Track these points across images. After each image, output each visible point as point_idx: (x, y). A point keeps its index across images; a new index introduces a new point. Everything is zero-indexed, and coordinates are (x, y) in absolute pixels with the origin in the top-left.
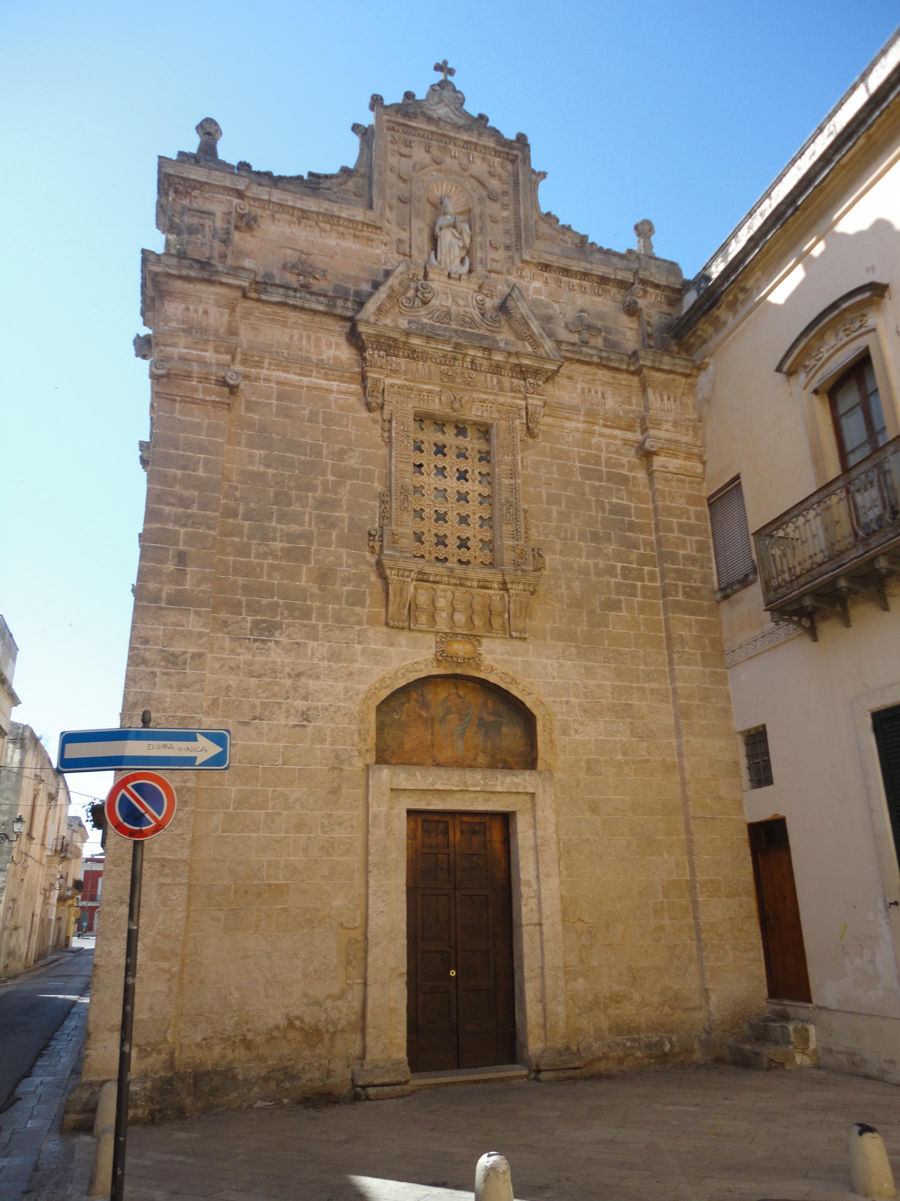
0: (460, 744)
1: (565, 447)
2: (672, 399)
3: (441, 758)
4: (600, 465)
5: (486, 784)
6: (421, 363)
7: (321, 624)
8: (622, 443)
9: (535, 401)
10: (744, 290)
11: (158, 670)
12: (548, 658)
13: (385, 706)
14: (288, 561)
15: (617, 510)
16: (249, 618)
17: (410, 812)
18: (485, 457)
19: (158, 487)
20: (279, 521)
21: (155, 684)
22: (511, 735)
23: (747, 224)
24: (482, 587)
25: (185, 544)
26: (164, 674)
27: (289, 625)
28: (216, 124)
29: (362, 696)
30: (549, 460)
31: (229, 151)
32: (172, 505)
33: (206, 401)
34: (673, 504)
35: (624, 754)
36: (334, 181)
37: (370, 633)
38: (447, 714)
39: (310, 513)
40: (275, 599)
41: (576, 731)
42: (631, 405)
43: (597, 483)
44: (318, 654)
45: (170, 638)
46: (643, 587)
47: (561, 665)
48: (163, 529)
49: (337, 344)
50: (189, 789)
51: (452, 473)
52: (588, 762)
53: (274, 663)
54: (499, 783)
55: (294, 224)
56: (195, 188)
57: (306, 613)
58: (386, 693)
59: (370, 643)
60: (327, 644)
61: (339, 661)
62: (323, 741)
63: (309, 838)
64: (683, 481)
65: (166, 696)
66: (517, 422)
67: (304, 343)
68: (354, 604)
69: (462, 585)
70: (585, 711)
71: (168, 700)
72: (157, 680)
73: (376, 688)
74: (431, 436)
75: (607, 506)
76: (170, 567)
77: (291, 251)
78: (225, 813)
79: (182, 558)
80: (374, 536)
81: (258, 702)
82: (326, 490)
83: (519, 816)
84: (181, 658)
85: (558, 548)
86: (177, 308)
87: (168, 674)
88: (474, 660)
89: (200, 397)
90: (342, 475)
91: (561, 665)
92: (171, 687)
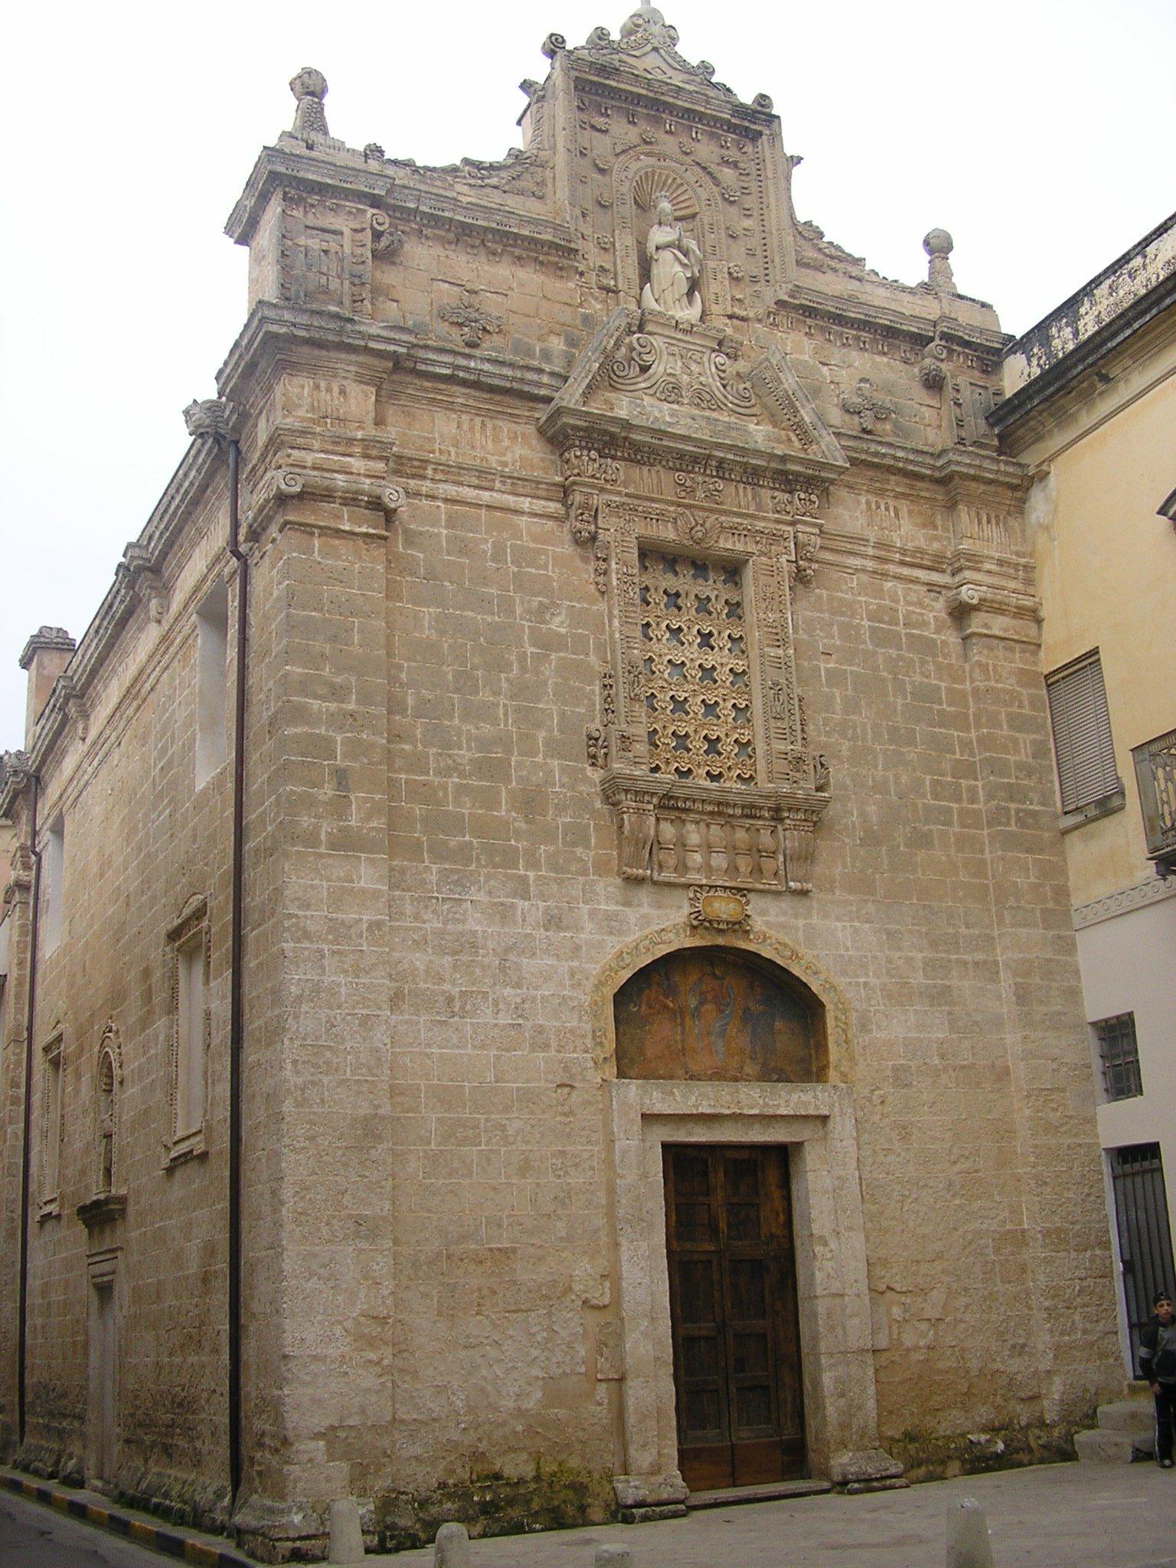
0: (720, 1046)
1: (848, 596)
2: (993, 521)
3: (694, 1068)
4: (897, 624)
5: (766, 1105)
6: (645, 469)
7: (531, 874)
8: (925, 588)
9: (806, 532)
10: (1105, 379)
11: (325, 947)
12: (838, 919)
13: (623, 997)
14: (480, 779)
15: (926, 694)
16: (434, 868)
17: (666, 1146)
18: (735, 610)
19: (299, 670)
20: (464, 718)
21: (323, 968)
22: (784, 1034)
23: (1108, 282)
24: (747, 816)
25: (345, 755)
26: (334, 952)
27: (488, 877)
28: (317, 73)
29: (593, 980)
30: (827, 615)
31: (350, 126)
32: (323, 698)
33: (355, 534)
34: (1000, 685)
35: (942, 1057)
36: (504, 174)
37: (600, 887)
38: (701, 1003)
39: (505, 705)
40: (467, 838)
41: (879, 1027)
42: (935, 528)
43: (893, 652)
44: (530, 919)
45: (338, 899)
46: (961, 810)
47: (856, 931)
48: (312, 734)
49: (523, 434)
50: (383, 1118)
51: (691, 636)
52: (895, 1069)
53: (474, 933)
54: (782, 1102)
55: (450, 243)
56: (312, 191)
57: (509, 859)
58: (626, 975)
59: (599, 903)
60: (541, 904)
61: (559, 928)
62: (546, 1047)
63: (538, 1185)
64: (1012, 650)
65: (339, 985)
66: (783, 559)
67: (478, 435)
68: (574, 844)
69: (720, 814)
70: (890, 996)
71: (343, 990)
72: (326, 963)
73: (611, 969)
74: (664, 581)
75: (909, 688)
76: (328, 791)
77: (447, 285)
78: (425, 1151)
79: (341, 778)
80: (596, 739)
81: (455, 991)
82: (523, 669)
83: (807, 1147)
84: (353, 930)
85: (845, 753)
86: (303, 387)
87: (339, 952)
88: (740, 926)
89: (347, 528)
90: (548, 643)
91: (856, 931)
92: (345, 971)
